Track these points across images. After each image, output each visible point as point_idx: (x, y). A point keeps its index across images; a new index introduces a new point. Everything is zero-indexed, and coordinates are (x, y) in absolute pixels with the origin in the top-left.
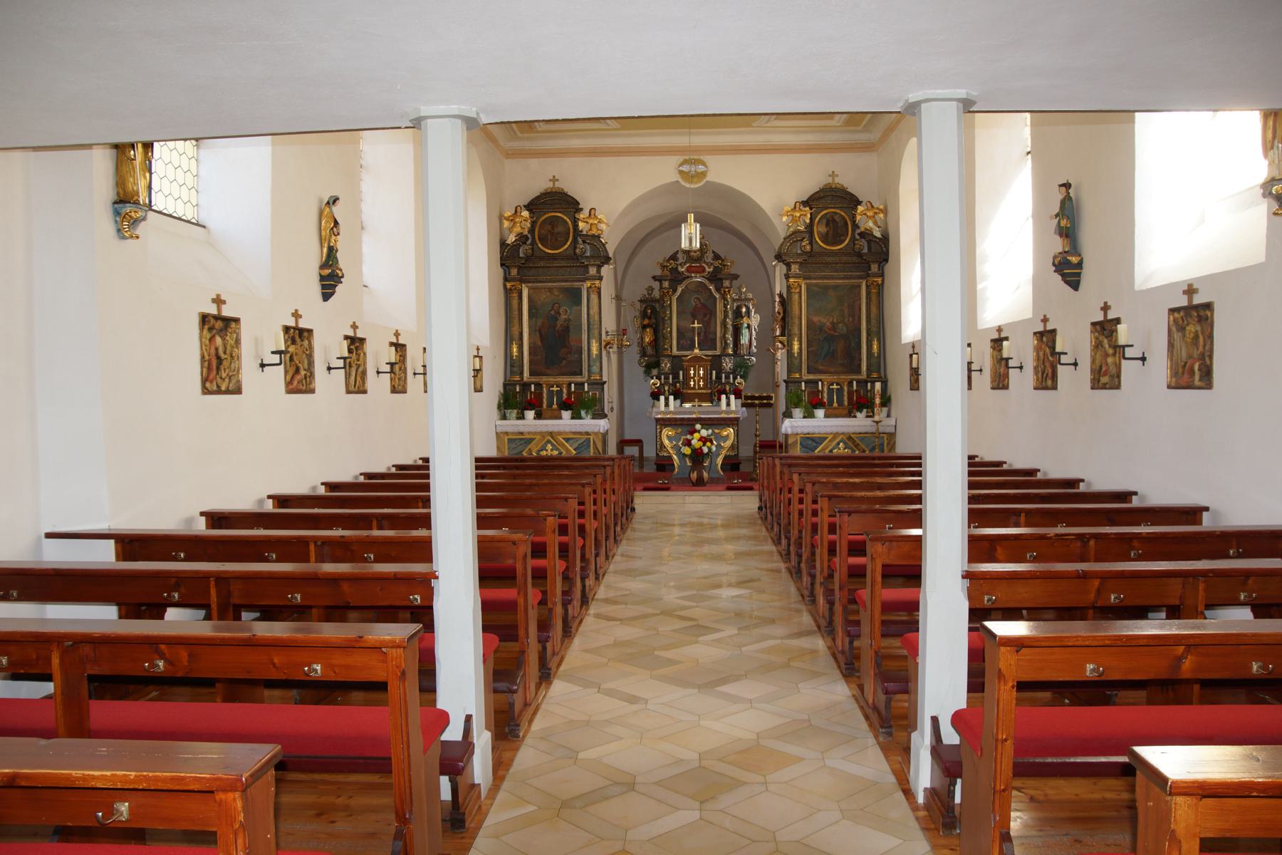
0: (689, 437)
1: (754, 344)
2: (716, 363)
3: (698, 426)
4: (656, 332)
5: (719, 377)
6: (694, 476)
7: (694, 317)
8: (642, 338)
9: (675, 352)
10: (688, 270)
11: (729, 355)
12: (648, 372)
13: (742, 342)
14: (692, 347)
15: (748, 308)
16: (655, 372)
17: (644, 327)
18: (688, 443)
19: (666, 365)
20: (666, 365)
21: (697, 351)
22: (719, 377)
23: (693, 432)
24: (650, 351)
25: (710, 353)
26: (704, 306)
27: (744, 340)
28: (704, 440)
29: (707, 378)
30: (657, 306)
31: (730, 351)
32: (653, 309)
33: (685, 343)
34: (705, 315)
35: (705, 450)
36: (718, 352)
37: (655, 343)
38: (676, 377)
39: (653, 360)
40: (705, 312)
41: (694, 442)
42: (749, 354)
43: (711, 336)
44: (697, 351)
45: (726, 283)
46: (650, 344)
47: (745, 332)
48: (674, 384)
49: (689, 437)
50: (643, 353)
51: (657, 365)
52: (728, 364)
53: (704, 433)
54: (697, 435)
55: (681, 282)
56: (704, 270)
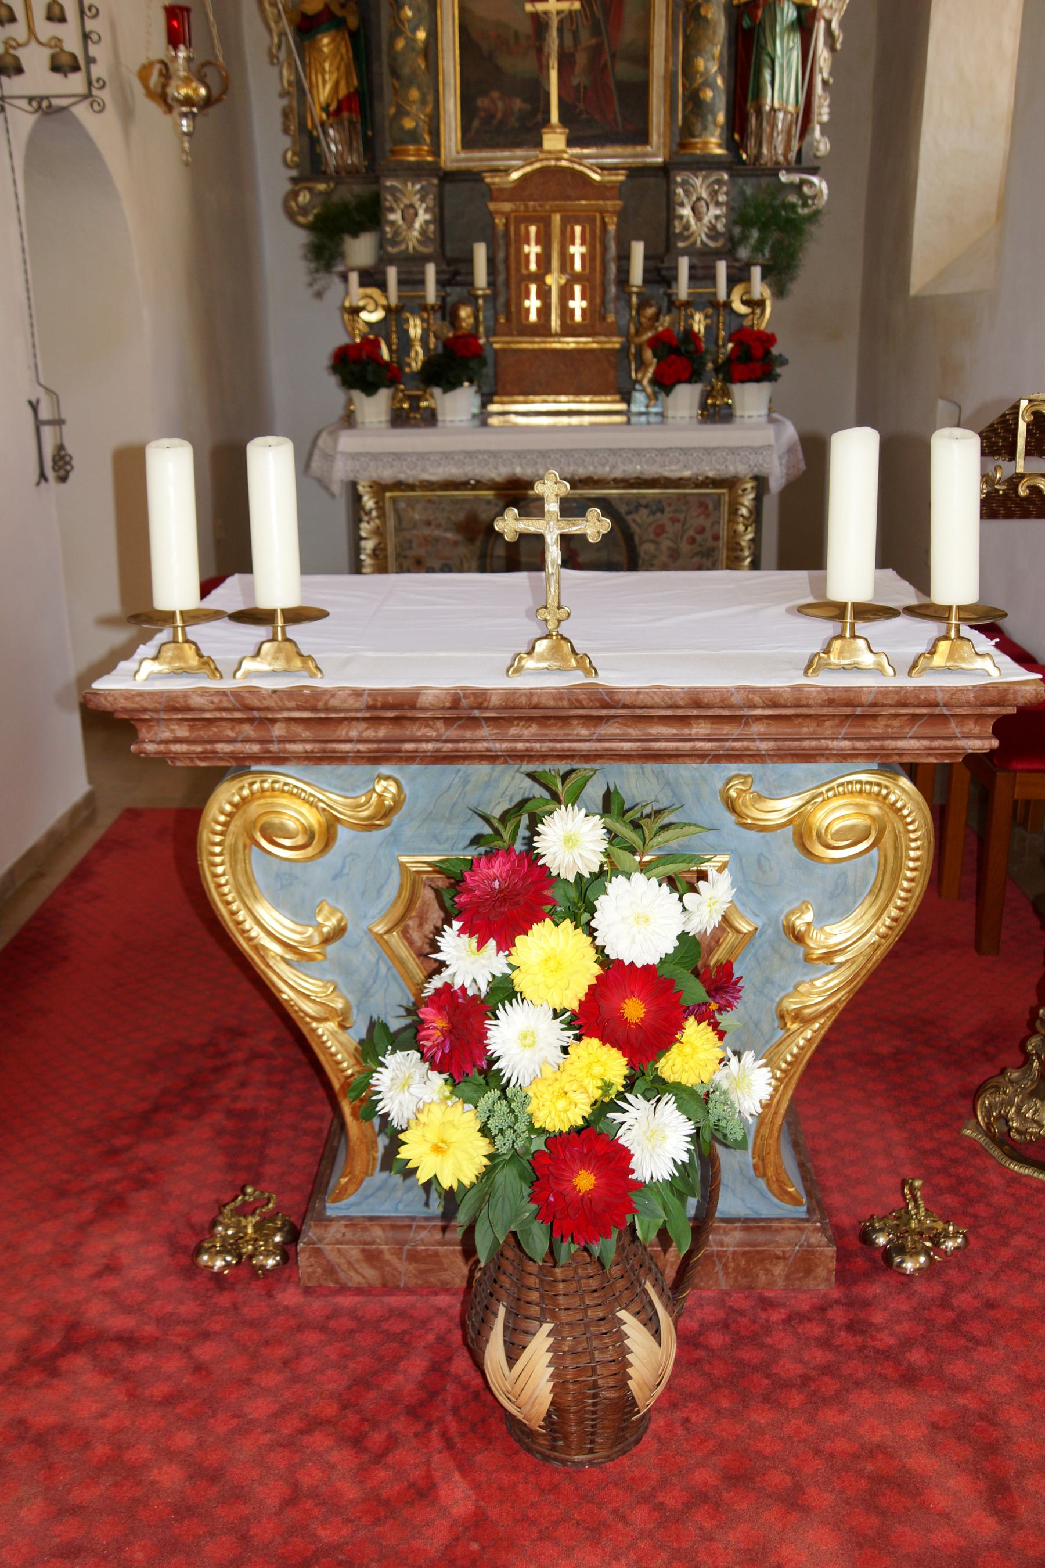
0: (467, 962)
1: (823, 112)
2: (648, 199)
3: (571, 840)
4: (363, 50)
5: (660, 274)
6: (528, 1376)
8: (299, 92)
11: (709, 164)
12: (324, 253)
13: (771, 98)
16: (361, 250)
17: (307, 27)
18: (458, 1039)
19: (412, 216)
20: (412, 216)
21: (554, 140)
22: (660, 274)
23: (510, 897)
24: (334, 146)
25: (616, 155)
27: (781, 91)
28: (635, 1012)
29: (604, 278)
31: (714, 145)
33: (502, 111)
35: (656, 1142)
36: (655, 154)
37: (360, 107)
38: (456, 273)
39: (351, 192)
41: (517, 1040)
42: (803, 163)
43: (623, 70)
44: (554, 140)
46: (336, 111)
47: (786, 49)
48: (447, 311)
49: (467, 962)
50: (310, 164)
51: (368, 215)
52: (701, 209)
53: (642, 923)
54: (553, 962)
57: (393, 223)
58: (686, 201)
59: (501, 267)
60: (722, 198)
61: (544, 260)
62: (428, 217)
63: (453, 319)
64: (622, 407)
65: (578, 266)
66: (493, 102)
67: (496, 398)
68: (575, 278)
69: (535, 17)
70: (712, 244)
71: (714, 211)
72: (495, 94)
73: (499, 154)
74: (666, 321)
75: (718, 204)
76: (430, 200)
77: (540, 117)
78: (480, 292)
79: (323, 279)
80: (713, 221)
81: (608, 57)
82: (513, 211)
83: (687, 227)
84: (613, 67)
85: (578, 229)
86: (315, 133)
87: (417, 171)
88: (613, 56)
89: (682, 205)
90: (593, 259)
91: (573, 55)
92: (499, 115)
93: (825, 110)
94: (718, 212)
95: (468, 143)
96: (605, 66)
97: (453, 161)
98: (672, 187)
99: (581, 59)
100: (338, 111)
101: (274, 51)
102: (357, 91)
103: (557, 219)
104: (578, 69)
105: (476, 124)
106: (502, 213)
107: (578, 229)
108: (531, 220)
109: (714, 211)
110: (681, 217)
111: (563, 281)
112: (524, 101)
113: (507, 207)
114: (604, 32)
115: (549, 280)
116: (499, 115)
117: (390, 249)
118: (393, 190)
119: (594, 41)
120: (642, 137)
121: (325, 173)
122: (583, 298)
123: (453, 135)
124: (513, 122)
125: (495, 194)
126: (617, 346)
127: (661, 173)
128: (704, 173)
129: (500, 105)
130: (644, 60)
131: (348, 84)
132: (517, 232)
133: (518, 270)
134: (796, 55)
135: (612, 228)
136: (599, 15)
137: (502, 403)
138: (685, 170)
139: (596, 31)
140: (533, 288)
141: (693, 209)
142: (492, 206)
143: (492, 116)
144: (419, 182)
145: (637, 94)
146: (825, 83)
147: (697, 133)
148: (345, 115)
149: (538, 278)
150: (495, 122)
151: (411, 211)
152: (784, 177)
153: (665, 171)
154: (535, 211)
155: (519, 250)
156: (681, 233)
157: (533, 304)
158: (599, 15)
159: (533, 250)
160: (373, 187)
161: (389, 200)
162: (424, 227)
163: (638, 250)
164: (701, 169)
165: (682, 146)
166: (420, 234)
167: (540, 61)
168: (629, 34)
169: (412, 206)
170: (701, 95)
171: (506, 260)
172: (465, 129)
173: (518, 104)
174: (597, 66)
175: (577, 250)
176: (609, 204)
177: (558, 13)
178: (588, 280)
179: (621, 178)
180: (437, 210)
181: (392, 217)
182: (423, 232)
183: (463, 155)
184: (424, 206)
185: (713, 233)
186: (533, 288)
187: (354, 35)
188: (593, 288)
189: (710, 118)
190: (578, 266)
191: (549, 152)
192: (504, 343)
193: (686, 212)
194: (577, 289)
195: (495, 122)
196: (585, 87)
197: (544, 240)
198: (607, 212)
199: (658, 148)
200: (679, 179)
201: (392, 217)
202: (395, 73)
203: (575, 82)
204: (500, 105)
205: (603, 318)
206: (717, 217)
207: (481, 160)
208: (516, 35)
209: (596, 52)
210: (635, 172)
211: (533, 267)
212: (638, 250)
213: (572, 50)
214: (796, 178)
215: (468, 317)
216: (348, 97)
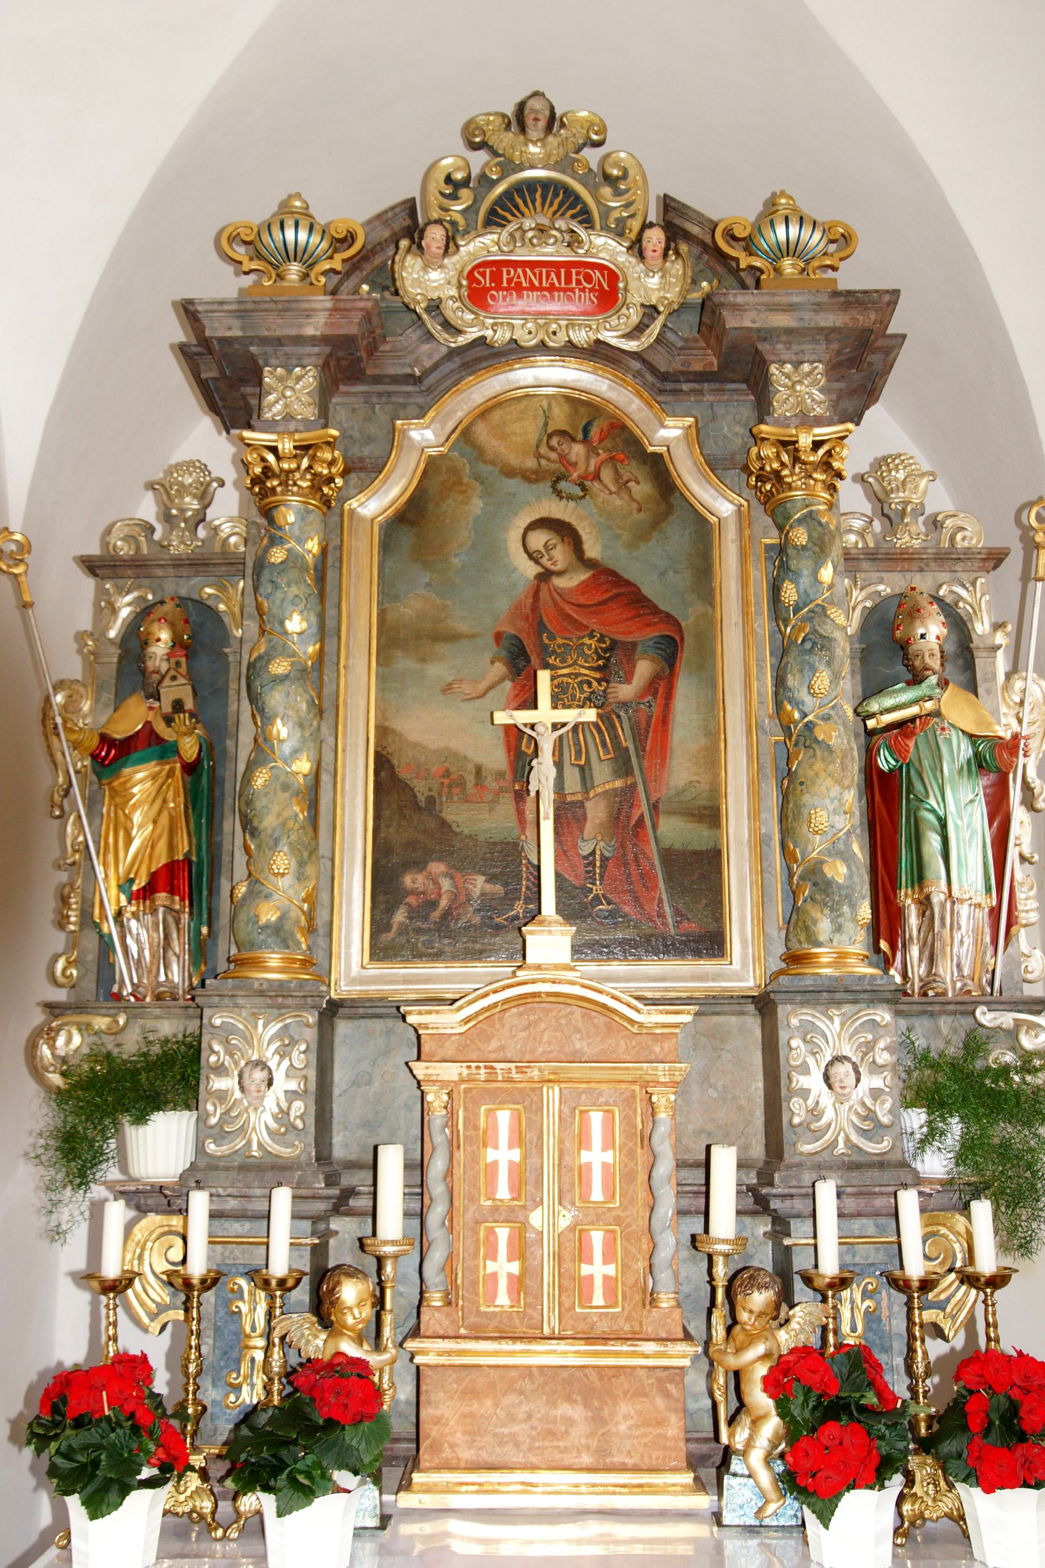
7: (520, 662)
9: (352, 965)
10: (483, 285)
14: (500, 927)
15: (959, 625)
16: (160, 1145)
19: (261, 1081)
21: (550, 943)
26: (613, 587)
30: (227, 598)
32: (201, 636)
34: (612, 660)
40: (626, 632)
43: (674, 831)
44: (550, 943)
45: (800, 386)
55: (423, 390)
56: (608, 293)
57: (222, 1096)
58: (811, 1061)
59: (436, 1188)
60: (883, 1057)
61: (525, 1179)
62: (293, 1085)
63: (323, 1309)
64: (704, 1502)
65: (597, 1194)
66: (434, 880)
67: (416, 1477)
68: (597, 1215)
69: (514, 734)
70: (871, 1147)
71: (871, 1081)
72: (437, 867)
73: (439, 969)
74: (799, 1328)
75: (876, 1068)
76: (298, 1058)
77: (519, 908)
78: (388, 1249)
79: (73, 1208)
80: (869, 1102)
81: (644, 808)
82: (462, 1081)
83: (815, 1113)
84: (655, 827)
85: (596, 1118)
86: (105, 929)
87: (276, 998)
88: (655, 808)
89: (805, 1070)
90: (628, 1177)
91: (581, 805)
92: (444, 903)
93: (1033, 904)
94: (877, 1082)
95: (381, 949)
96: (641, 821)
97: (353, 981)
98: (783, 1035)
99: (596, 812)
100: (146, 893)
101: (57, 798)
102: (187, 861)
103: (552, 1095)
104: (589, 828)
105: (400, 916)
106: (443, 1084)
107: (596, 1118)
108: (499, 1097)
109: (871, 1081)
110: (805, 1093)
111: (565, 1221)
112: (492, 879)
113: (451, 1072)
114: (637, 771)
115: (536, 1218)
116: (444, 903)
117: (211, 1147)
118: (226, 1033)
119: (619, 784)
120: (711, 943)
121: (118, 997)
122: (608, 1257)
123: (356, 936)
124: (470, 916)
125: (426, 1048)
126: (686, 1362)
127: (751, 1008)
128: (847, 1009)
129: (446, 884)
130: (711, 815)
131: (171, 847)
132: (471, 1123)
133: (473, 1199)
134: (979, 812)
135: (662, 1115)
136: (628, 743)
137: (428, 1489)
138: (804, 1003)
139: (623, 765)
140: (503, 1234)
141: (827, 1078)
142: (420, 1069)
143: (433, 904)
144: (280, 1017)
145: (699, 873)
146: (1023, 858)
147: (822, 937)
148: (162, 897)
149: (514, 1215)
150: (436, 915)
151: (259, 1075)
152: (985, 1017)
153: (764, 1004)
154: (511, 1080)
155: (474, 1160)
156: (806, 1125)
157: (504, 1267)
158: (628, 743)
159: (503, 1155)
160: (193, 1026)
161: (215, 1053)
162: (284, 1105)
163: (725, 1164)
164: (839, 1003)
165: (795, 959)
166: (275, 1117)
167: (520, 813)
168: (681, 772)
169: (261, 1064)
170: (828, 871)
171: (449, 1172)
172: (379, 925)
173: (479, 884)
174: (626, 825)
175: (597, 1157)
176: (661, 1071)
177: (555, 727)
178: (618, 1221)
179: (687, 1018)
180: (312, 1074)
181: (219, 1084)
182: (282, 1115)
183: (376, 970)
184: (286, 1063)
185: (866, 1126)
186: (503, 1234)
187: (191, 769)
188: (627, 1237)
189: (846, 909)
190: (597, 1194)
191: (538, 967)
192: (440, 1354)
193: (813, 1081)
194: (597, 1238)
195: (436, 915)
196: (604, 859)
197: (527, 1138)
198: (658, 1083)
199: (744, 964)
200: (794, 1022)
201: (219, 1084)
202: (249, 826)
203: (585, 849)
204: (446, 884)
205: (653, 1302)
206: (876, 1094)
207: (407, 980)
208: (479, 770)
209: (622, 801)
210: (710, 1005)
211: (503, 1192)
212: (725, 1164)
213: (579, 797)
214: (1007, 1019)
215: (359, 1305)
216: (171, 867)
